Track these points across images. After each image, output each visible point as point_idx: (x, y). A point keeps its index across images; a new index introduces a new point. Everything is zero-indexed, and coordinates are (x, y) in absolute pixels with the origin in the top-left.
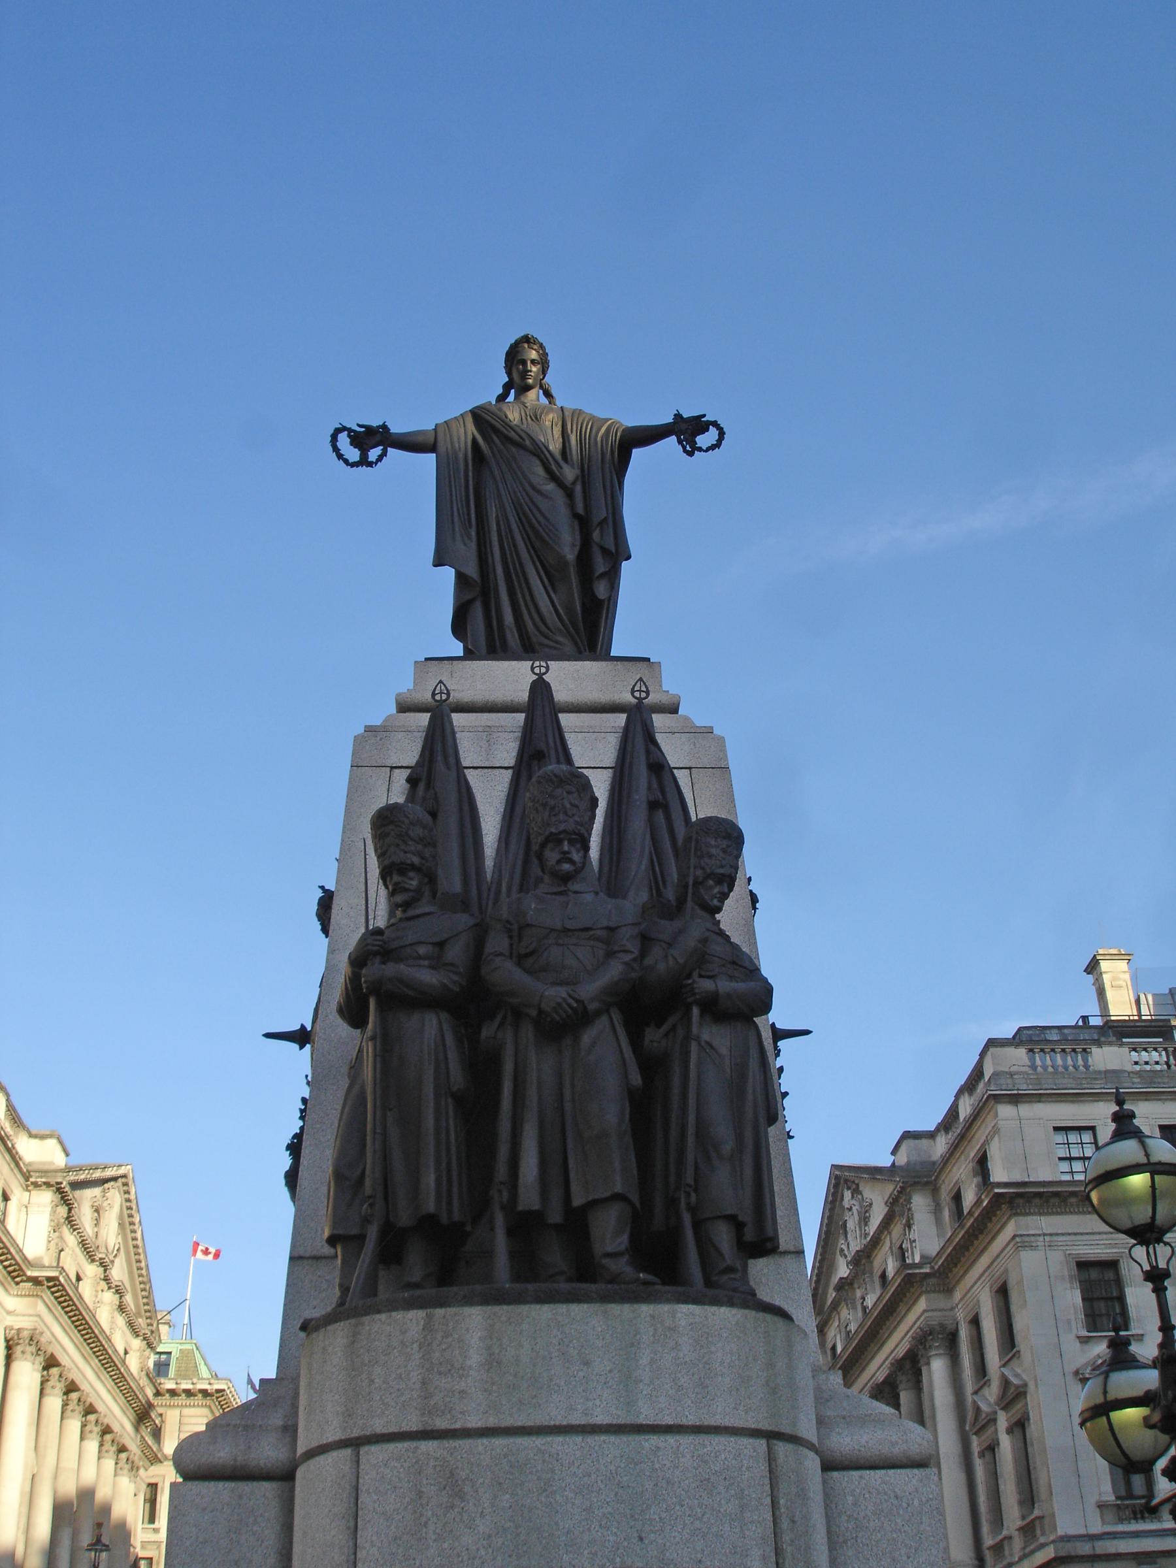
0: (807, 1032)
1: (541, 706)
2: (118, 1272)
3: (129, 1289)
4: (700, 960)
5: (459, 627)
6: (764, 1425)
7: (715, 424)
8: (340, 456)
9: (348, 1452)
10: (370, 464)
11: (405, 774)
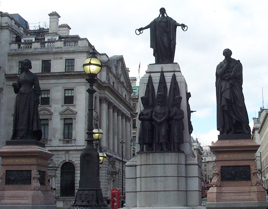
0: (196, 111)
1: (162, 73)
2: (122, 79)
3: (124, 82)
4: (175, 114)
5: (154, 55)
6: (177, 163)
8: (137, 34)
9: (140, 166)
10: (141, 33)
11: (146, 84)
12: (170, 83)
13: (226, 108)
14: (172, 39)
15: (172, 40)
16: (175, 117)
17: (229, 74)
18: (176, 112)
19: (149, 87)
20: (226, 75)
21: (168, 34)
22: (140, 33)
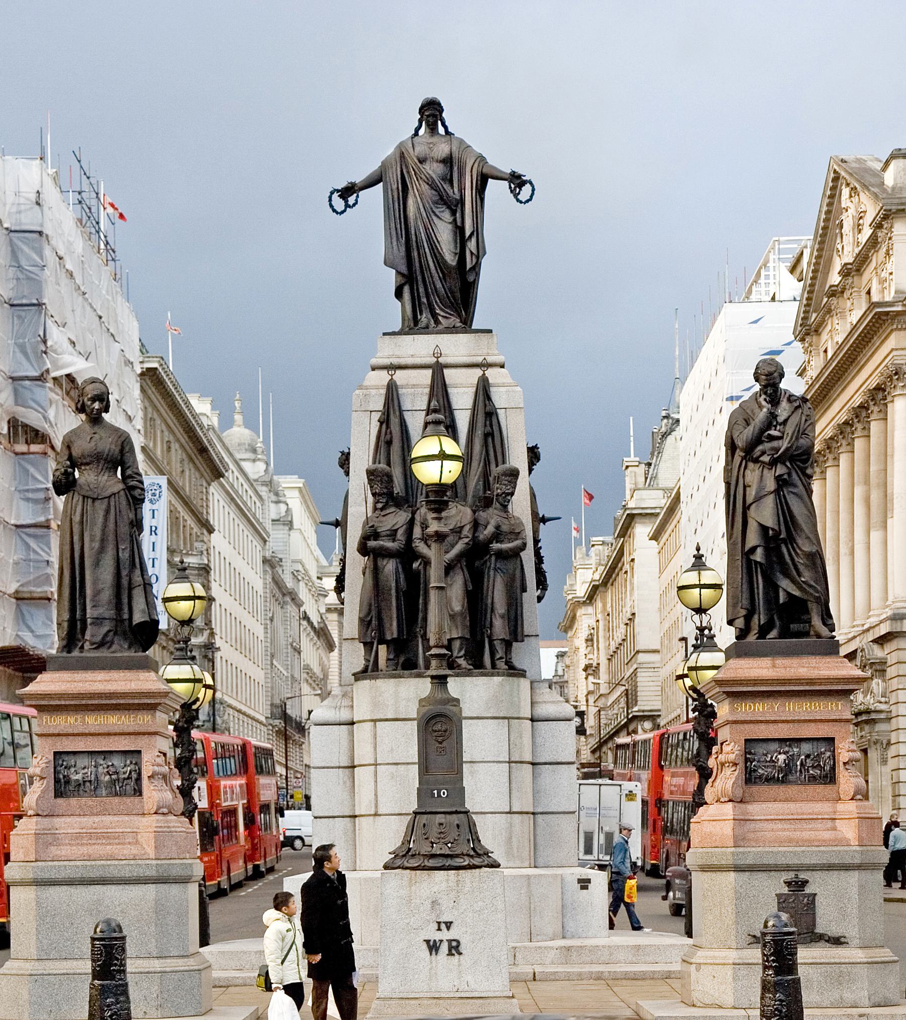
1: (438, 369)
7: (531, 183)
10: (350, 207)
12: (469, 413)
13: (759, 556)
14: (468, 234)
15: (472, 234)
16: (496, 546)
17: (775, 444)
18: (498, 527)
19: (388, 427)
20: (760, 448)
21: (454, 213)
22: (347, 206)
